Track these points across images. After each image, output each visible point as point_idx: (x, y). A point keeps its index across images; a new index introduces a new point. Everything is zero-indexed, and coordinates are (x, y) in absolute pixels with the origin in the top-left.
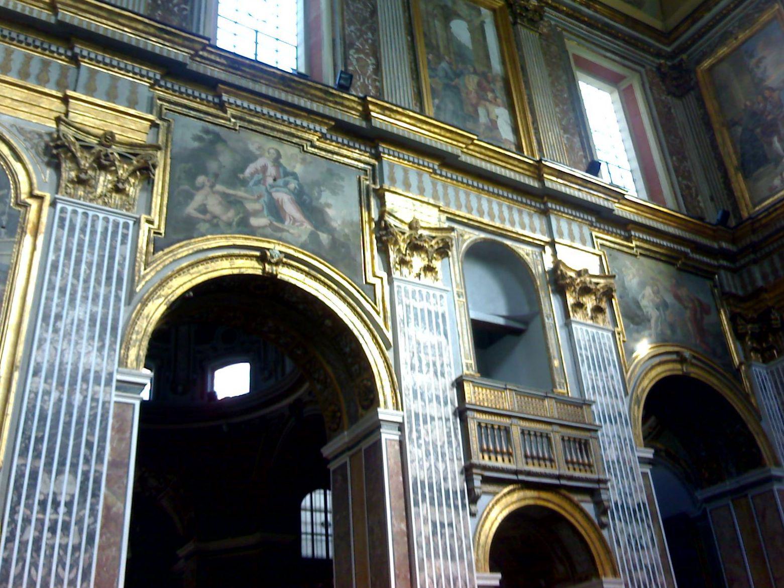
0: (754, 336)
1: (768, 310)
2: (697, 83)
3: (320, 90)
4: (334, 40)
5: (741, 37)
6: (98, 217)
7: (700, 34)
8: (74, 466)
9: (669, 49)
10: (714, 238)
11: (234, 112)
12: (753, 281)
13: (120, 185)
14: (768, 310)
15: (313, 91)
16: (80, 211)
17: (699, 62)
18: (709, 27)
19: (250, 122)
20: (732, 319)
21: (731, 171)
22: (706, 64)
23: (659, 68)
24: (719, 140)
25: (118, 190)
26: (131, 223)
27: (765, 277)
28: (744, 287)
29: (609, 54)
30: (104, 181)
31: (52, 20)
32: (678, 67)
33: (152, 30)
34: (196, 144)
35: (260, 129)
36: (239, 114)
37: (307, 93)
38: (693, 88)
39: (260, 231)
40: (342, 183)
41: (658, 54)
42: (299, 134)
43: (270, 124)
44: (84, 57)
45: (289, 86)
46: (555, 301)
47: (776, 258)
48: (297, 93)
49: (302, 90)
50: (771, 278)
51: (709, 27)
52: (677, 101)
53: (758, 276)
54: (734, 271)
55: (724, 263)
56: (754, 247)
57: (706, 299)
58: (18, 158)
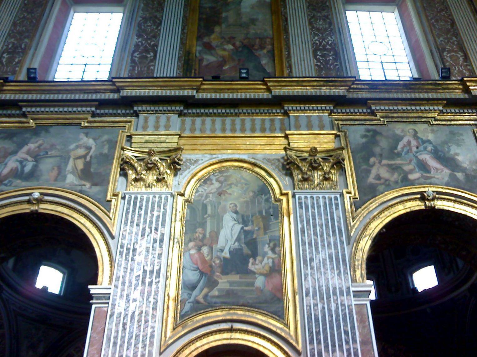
3: (431, 84)
6: (319, 197)
8: (341, 346)
11: (381, 114)
13: (327, 176)
15: (427, 87)
16: (309, 196)
19: (393, 117)
25: (326, 179)
26: (338, 196)
30: (317, 176)
31: (270, 97)
33: (322, 83)
34: (364, 140)
35: (400, 119)
36: (384, 115)
37: (422, 89)
39: (417, 181)
40: (461, 137)
42: (425, 115)
43: (405, 115)
44: (290, 110)
45: (410, 89)
48: (417, 91)
49: (419, 89)
58: (271, 176)
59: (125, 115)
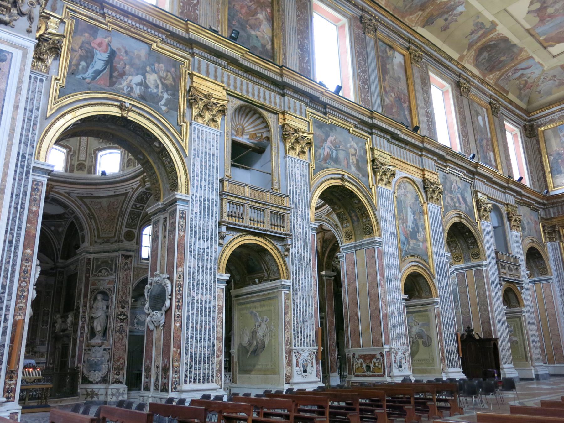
0: (549, 233)
1: (555, 226)
2: (538, 135)
4: (459, 134)
5: (559, 123)
7: (542, 117)
9: (528, 118)
10: (542, 199)
12: (550, 214)
14: (555, 226)
17: (539, 126)
18: (547, 115)
20: (543, 227)
21: (547, 173)
22: (542, 129)
23: (525, 126)
24: (544, 160)
27: (554, 213)
28: (546, 215)
29: (513, 123)
32: (532, 126)
38: (535, 136)
41: (525, 120)
46: (508, 223)
47: (560, 208)
50: (557, 214)
51: (547, 115)
52: (529, 140)
53: (552, 212)
54: (543, 209)
55: (542, 206)
56: (553, 203)
57: (537, 220)
59: (366, 132)
